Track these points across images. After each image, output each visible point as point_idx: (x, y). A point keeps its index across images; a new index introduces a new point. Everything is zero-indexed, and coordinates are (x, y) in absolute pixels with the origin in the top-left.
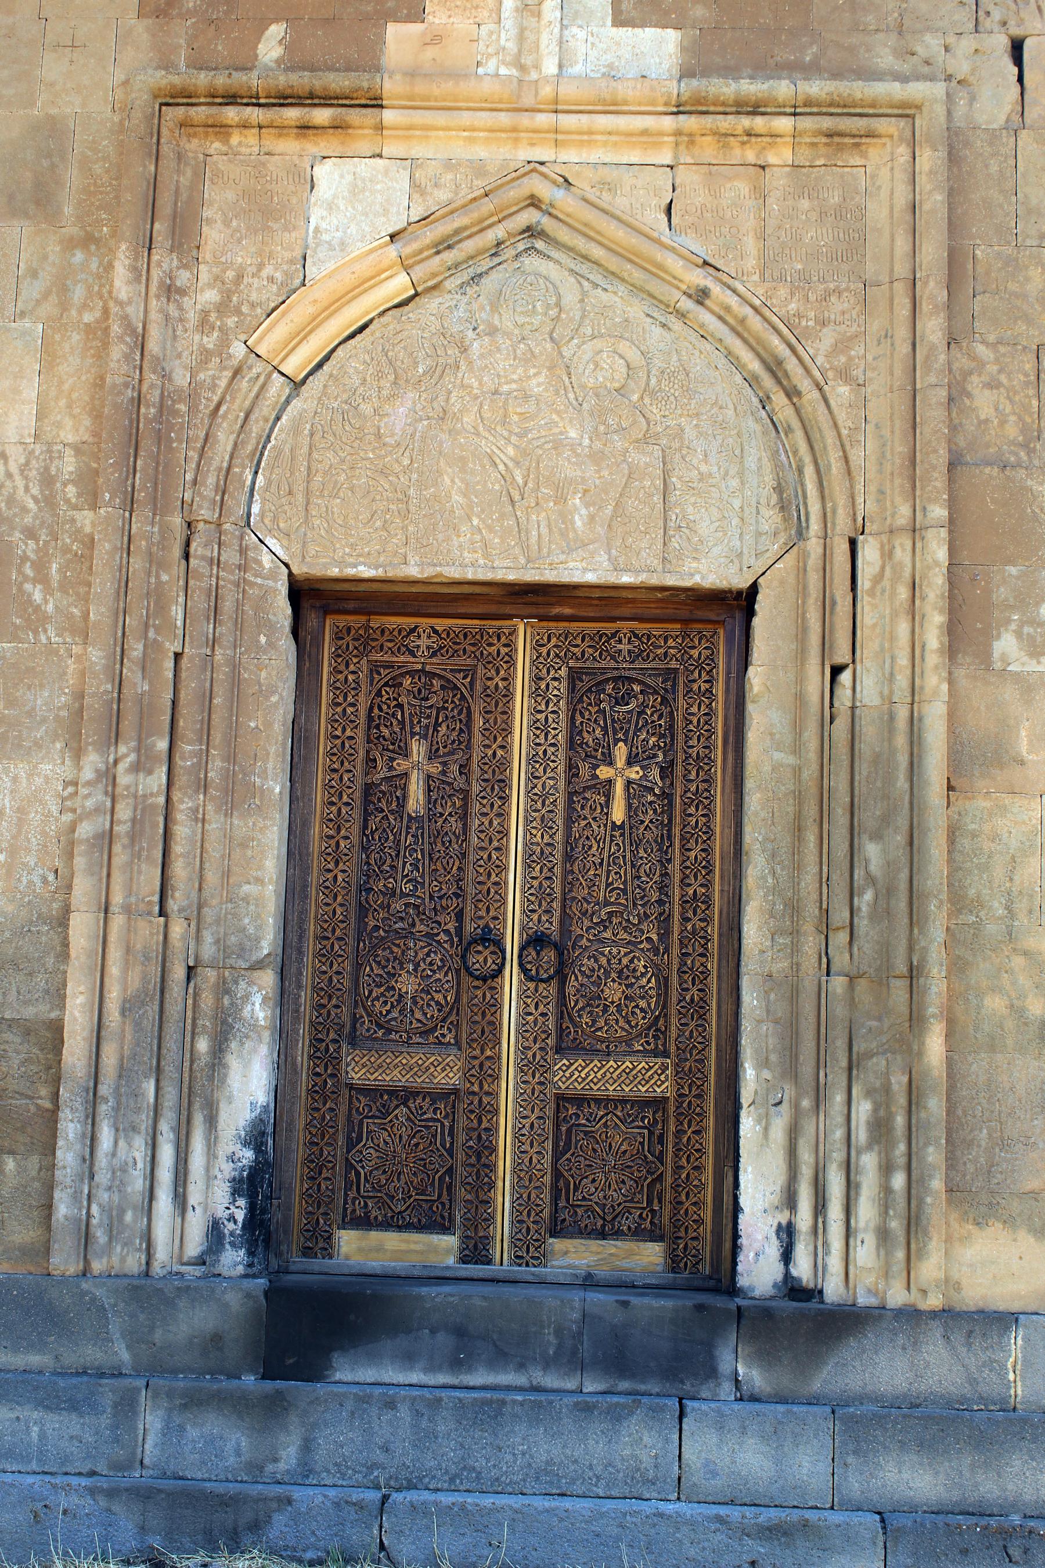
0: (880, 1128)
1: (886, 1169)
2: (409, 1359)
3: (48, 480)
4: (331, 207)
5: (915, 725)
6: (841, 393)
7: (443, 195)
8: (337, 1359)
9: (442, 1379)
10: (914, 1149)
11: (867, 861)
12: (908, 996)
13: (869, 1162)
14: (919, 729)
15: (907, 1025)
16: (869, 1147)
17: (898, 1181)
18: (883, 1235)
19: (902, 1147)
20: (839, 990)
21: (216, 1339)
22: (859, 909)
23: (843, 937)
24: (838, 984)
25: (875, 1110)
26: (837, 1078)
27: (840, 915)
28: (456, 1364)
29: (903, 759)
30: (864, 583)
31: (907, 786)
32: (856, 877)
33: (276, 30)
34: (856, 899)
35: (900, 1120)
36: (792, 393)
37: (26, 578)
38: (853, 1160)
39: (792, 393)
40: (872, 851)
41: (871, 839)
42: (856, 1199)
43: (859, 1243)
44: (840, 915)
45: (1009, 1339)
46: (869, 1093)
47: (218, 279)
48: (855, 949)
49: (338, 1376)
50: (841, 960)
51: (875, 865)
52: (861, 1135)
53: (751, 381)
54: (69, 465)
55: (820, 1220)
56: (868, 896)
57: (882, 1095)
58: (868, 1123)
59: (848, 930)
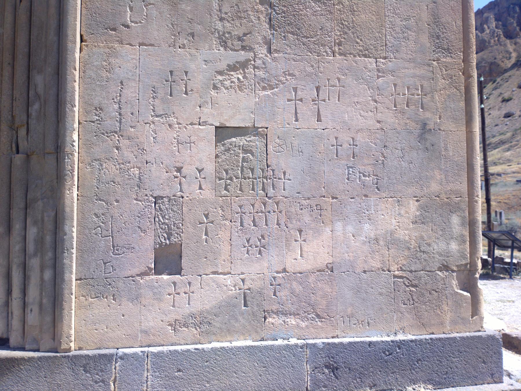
1: (42, 269)
10: (57, 256)
11: (36, 86)
12: (56, 164)
14: (63, 4)
15: (55, 181)
16: (35, 255)
17: (48, 275)
19: (50, 254)
20: (19, 163)
22: (31, 114)
23: (22, 132)
24: (18, 159)
25: (38, 233)
26: (17, 215)
27: (20, 118)
29: (53, 23)
31: (56, 38)
32: (30, 95)
34: (30, 108)
35: (48, 239)
38: (27, 262)
40: (39, 80)
41: (38, 73)
42: (28, 285)
43: (29, 311)
44: (20, 118)
45: (111, 367)
46: (35, 223)
48: (29, 138)
50: (23, 145)
51: (40, 89)
52: (31, 247)
55: (10, 298)
56: (36, 106)
58: (35, 240)
59: (26, 126)
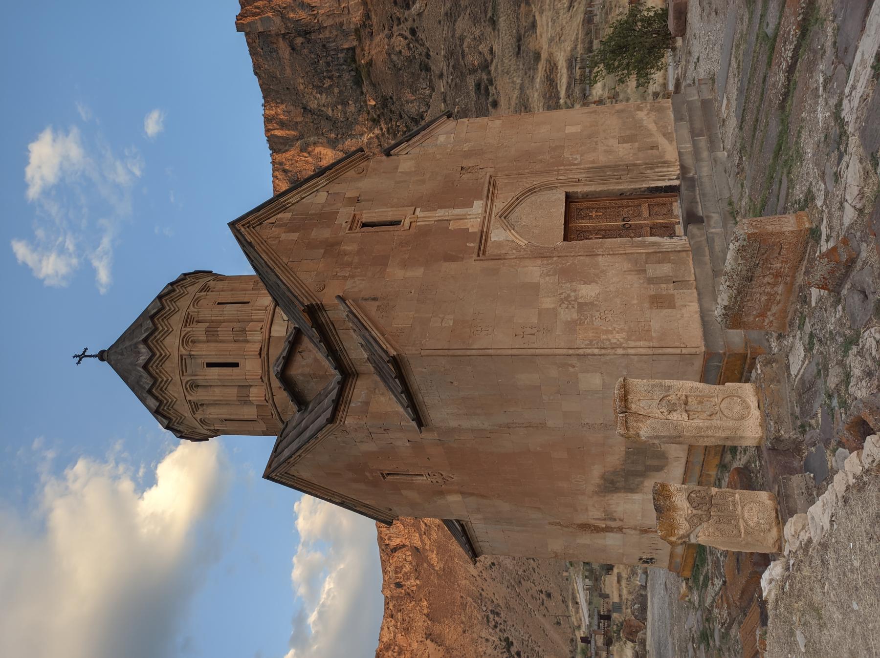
0: (651, 169)
1: (658, 167)
2: (697, 208)
3: (548, 264)
4: (499, 238)
5: (589, 168)
6: (535, 183)
7: (499, 226)
8: (698, 215)
9: (700, 204)
13: (657, 170)
18: (668, 167)
21: (698, 228)
28: (697, 202)
30: (566, 178)
33: (468, 244)
36: (534, 188)
37: (566, 264)
39: (534, 188)
47: (511, 250)
49: (701, 215)
53: (531, 194)
54: (545, 262)
57: (646, 169)
